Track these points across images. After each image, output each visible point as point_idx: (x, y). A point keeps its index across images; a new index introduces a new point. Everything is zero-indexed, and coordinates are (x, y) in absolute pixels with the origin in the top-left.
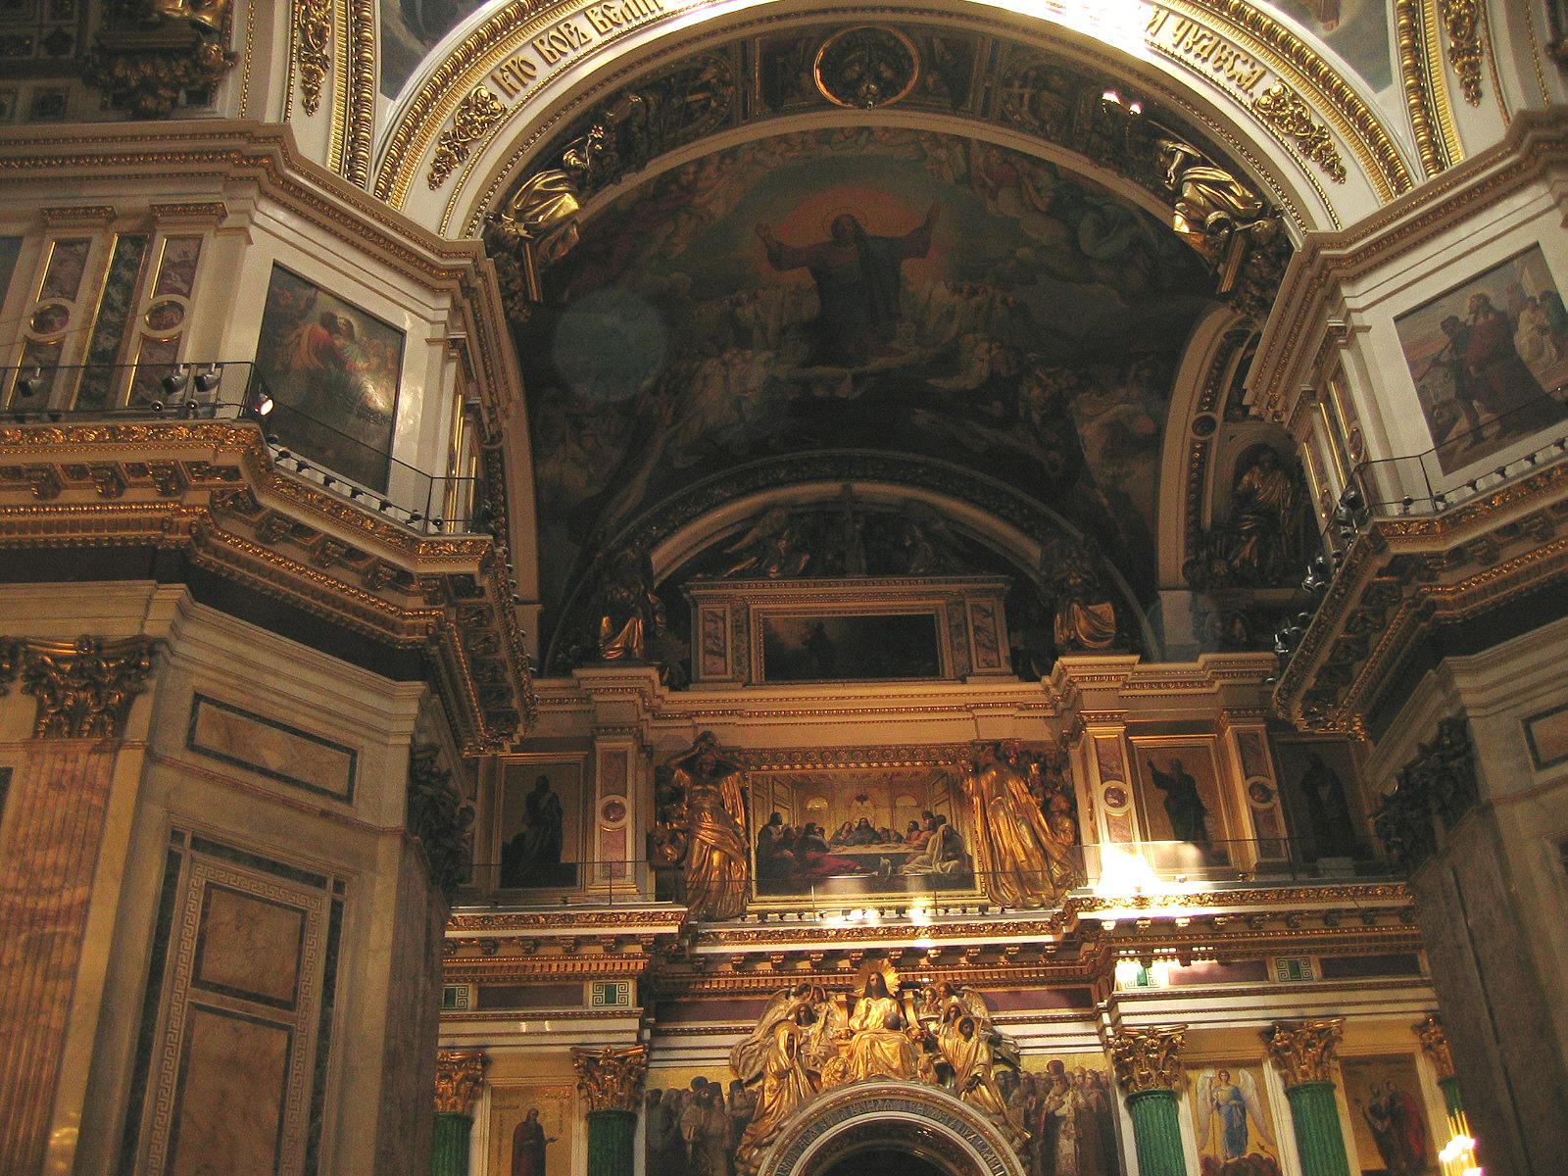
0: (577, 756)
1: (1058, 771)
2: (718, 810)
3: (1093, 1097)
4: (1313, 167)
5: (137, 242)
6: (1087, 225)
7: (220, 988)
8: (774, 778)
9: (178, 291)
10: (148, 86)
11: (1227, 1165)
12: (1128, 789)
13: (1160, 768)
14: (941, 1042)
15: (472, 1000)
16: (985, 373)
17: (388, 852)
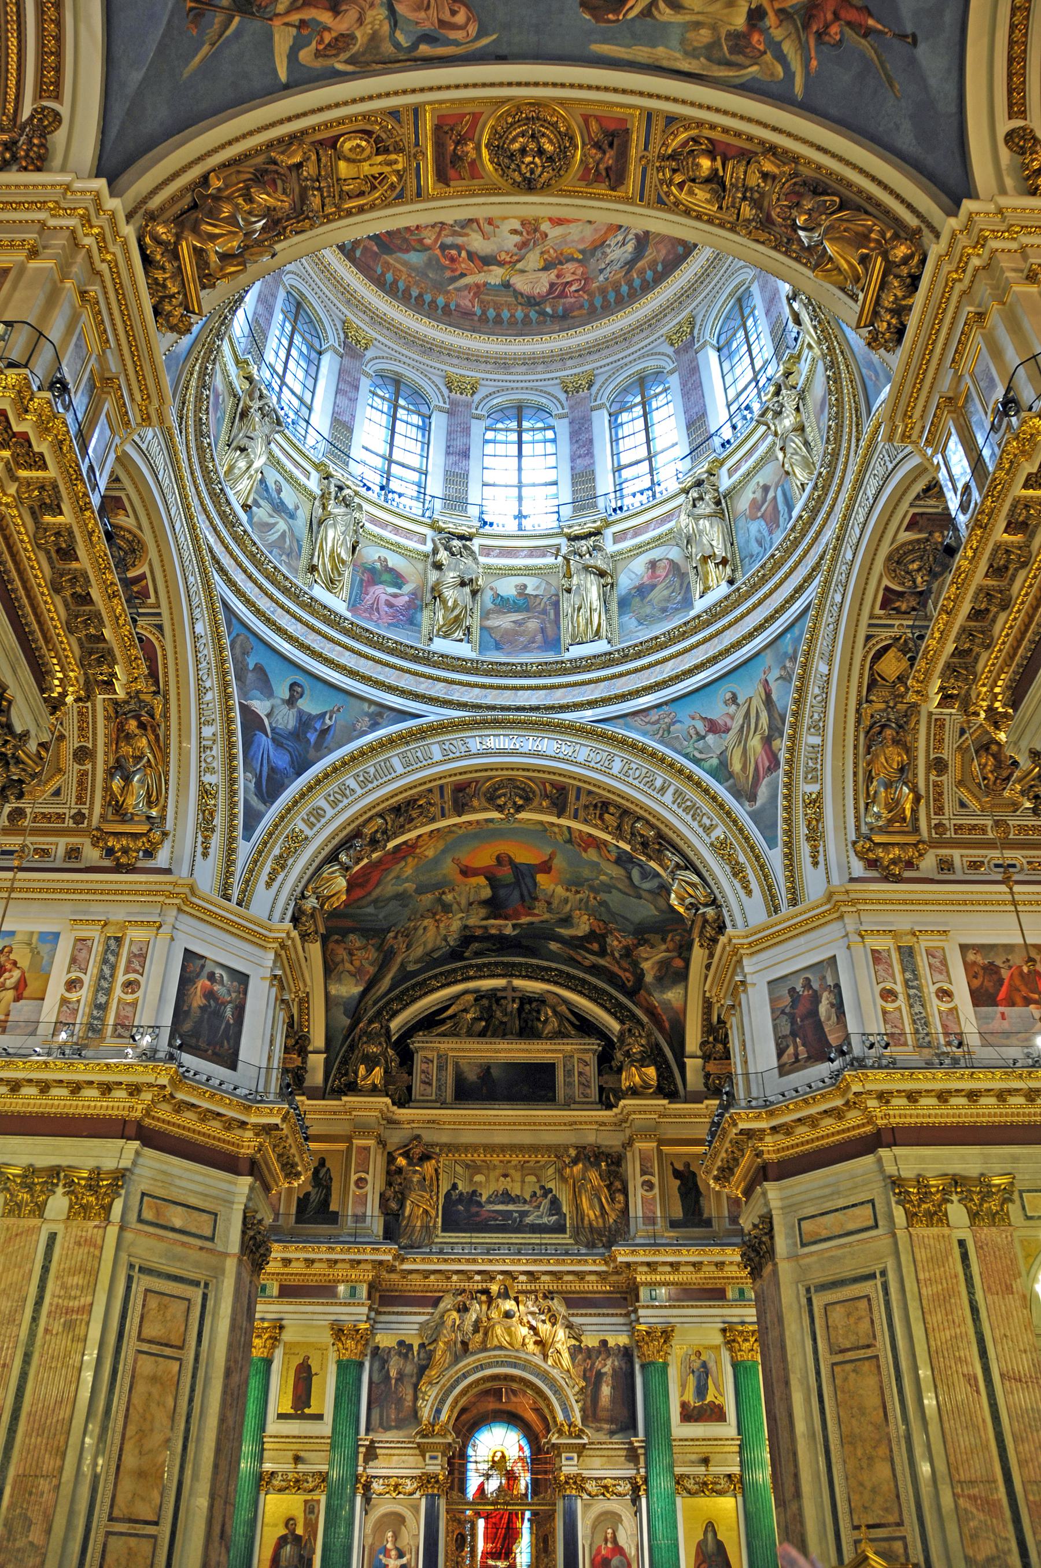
0: (342, 1146)
4: (738, 886)
5: (118, 940)
6: (636, 873)
7: (150, 1342)
9: (135, 971)
10: (125, 851)
12: (655, 1180)
15: (275, 1292)
16: (587, 928)
17: (231, 1265)
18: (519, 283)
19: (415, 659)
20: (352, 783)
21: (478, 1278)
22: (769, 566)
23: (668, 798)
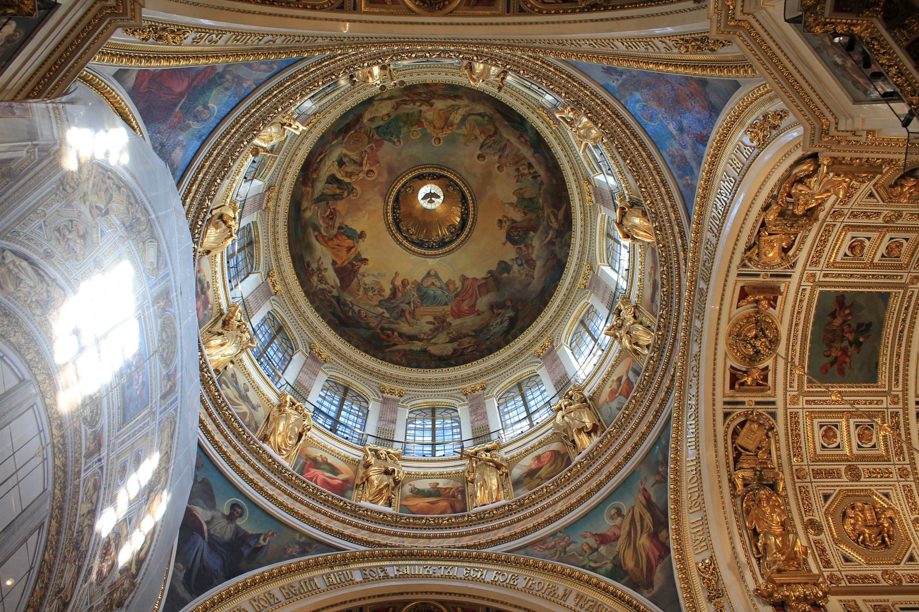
18: (433, 350)
19: (343, 510)
20: (278, 595)
22: (631, 406)
23: (571, 602)
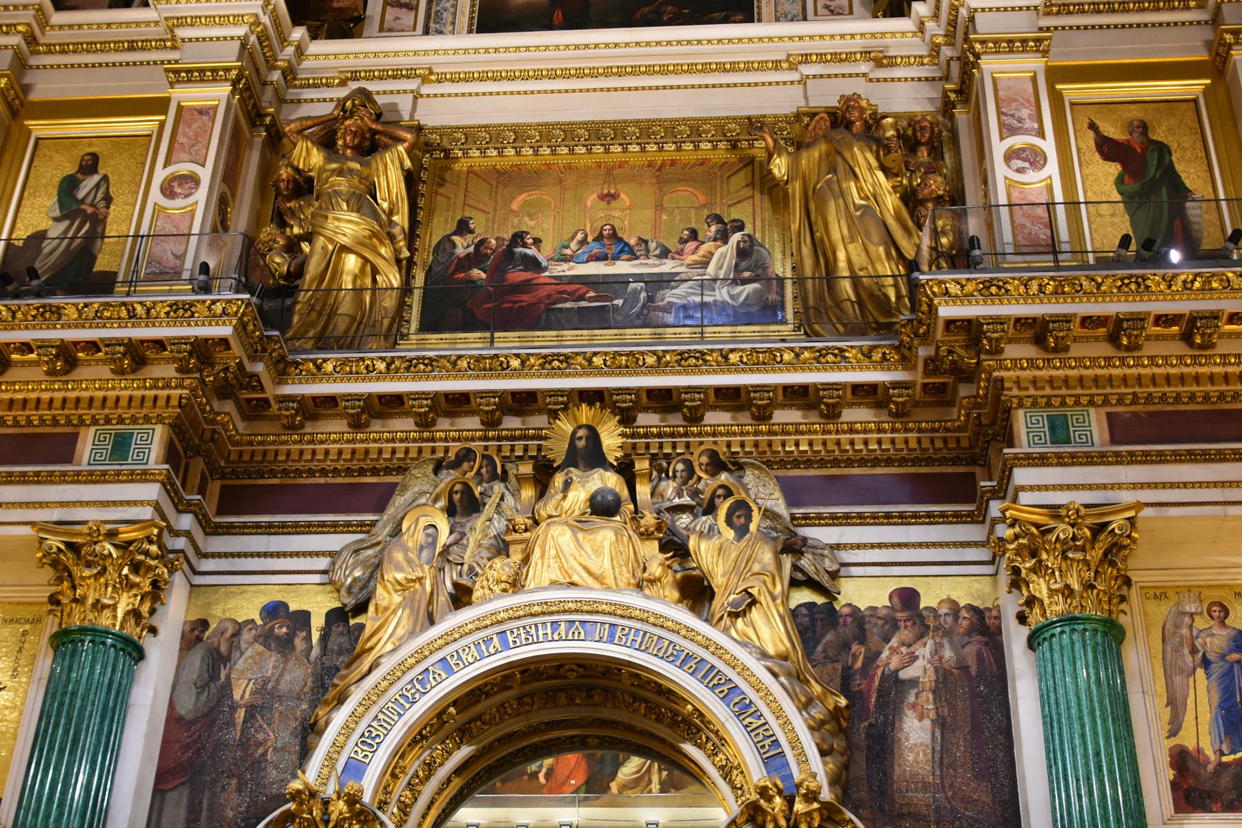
1: (936, 152)
2: (364, 199)
3: (970, 651)
8: (470, 171)
11: (1222, 766)
13: (1112, 130)
14: (692, 544)
21: (511, 423)
